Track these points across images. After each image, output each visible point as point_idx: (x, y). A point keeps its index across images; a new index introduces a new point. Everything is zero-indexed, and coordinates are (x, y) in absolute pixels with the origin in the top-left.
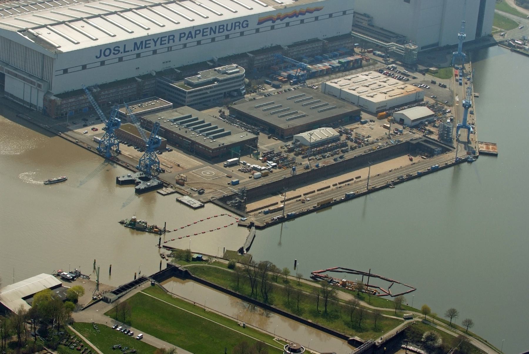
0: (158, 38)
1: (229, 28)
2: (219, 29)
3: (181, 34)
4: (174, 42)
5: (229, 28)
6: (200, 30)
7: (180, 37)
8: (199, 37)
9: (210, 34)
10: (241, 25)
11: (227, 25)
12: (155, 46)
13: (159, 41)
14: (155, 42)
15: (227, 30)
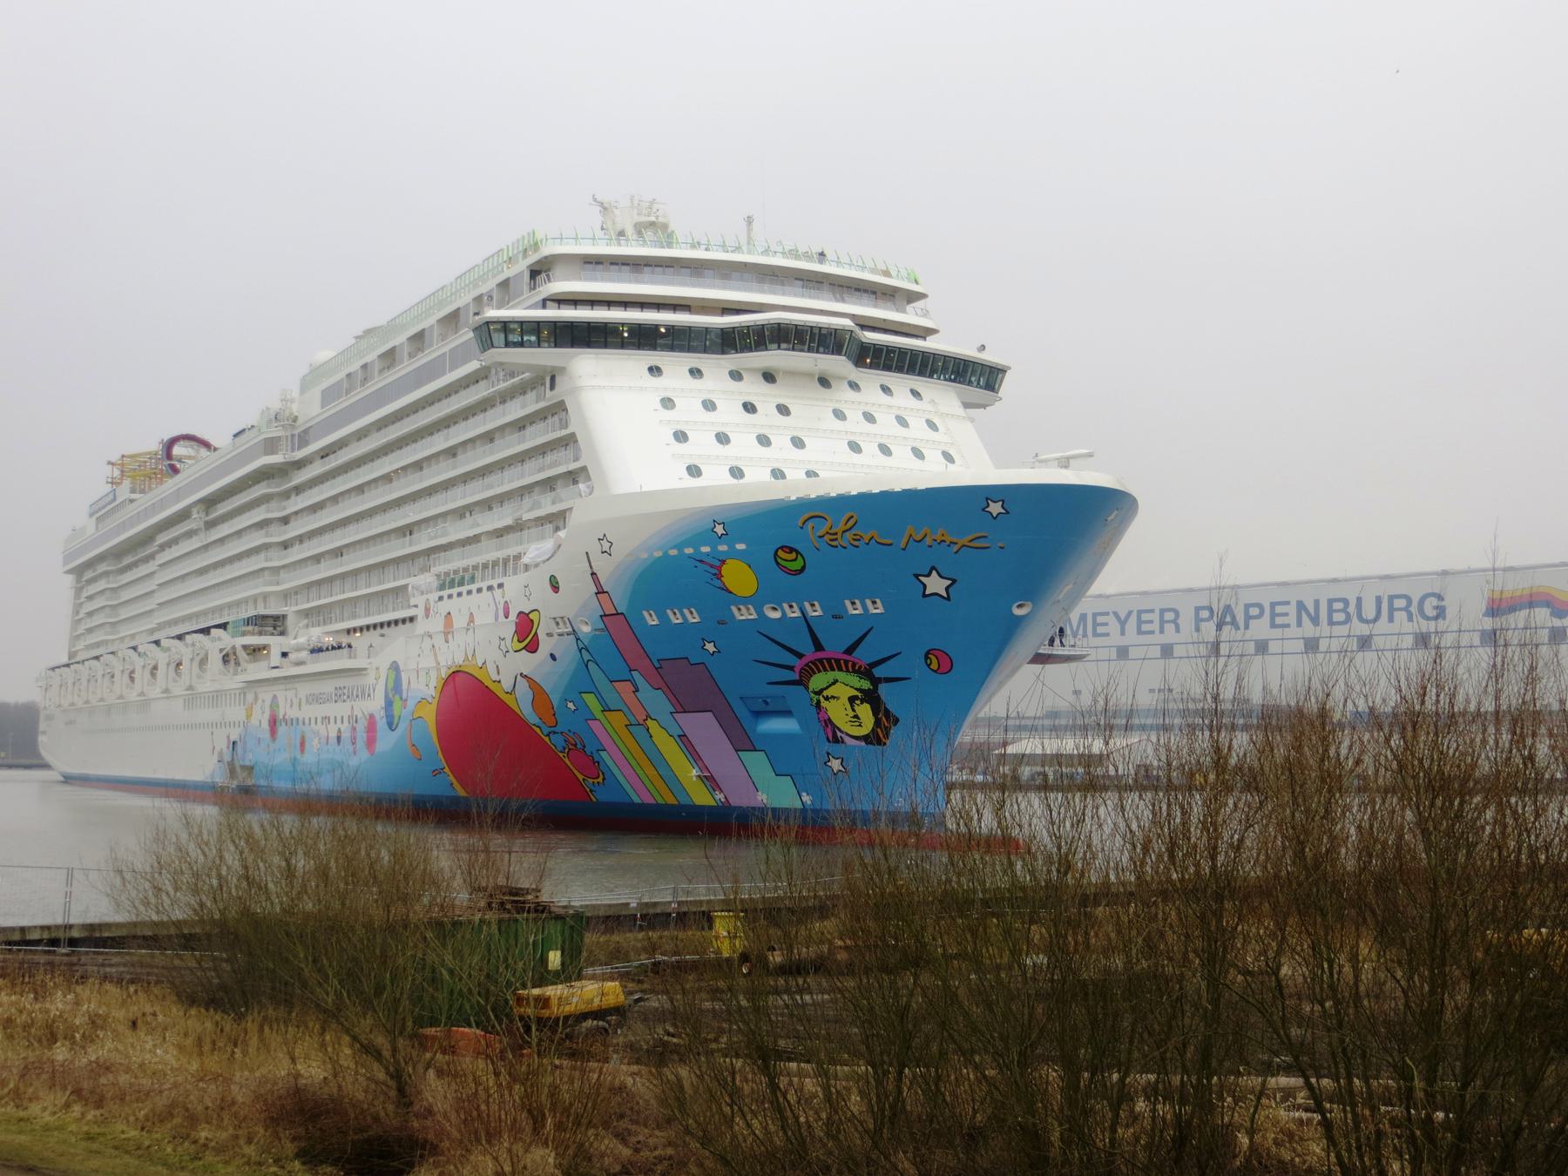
0: (1130, 613)
1: (1369, 612)
2: (1331, 611)
3: (1198, 609)
4: (1178, 630)
5: (1369, 612)
6: (1260, 606)
7: (1198, 620)
8: (1260, 629)
9: (1299, 624)
10: (1414, 609)
11: (1359, 600)
12: (1123, 633)
13: (1133, 621)
14: (1123, 623)
15: (1361, 620)
